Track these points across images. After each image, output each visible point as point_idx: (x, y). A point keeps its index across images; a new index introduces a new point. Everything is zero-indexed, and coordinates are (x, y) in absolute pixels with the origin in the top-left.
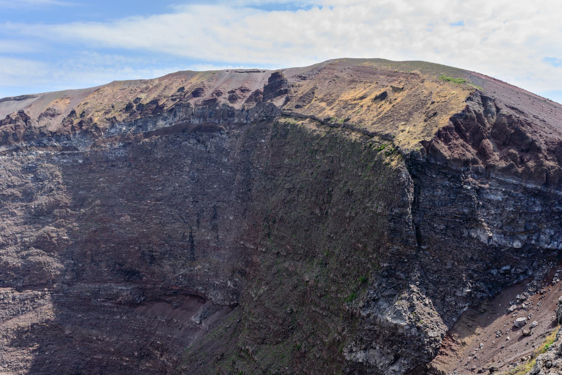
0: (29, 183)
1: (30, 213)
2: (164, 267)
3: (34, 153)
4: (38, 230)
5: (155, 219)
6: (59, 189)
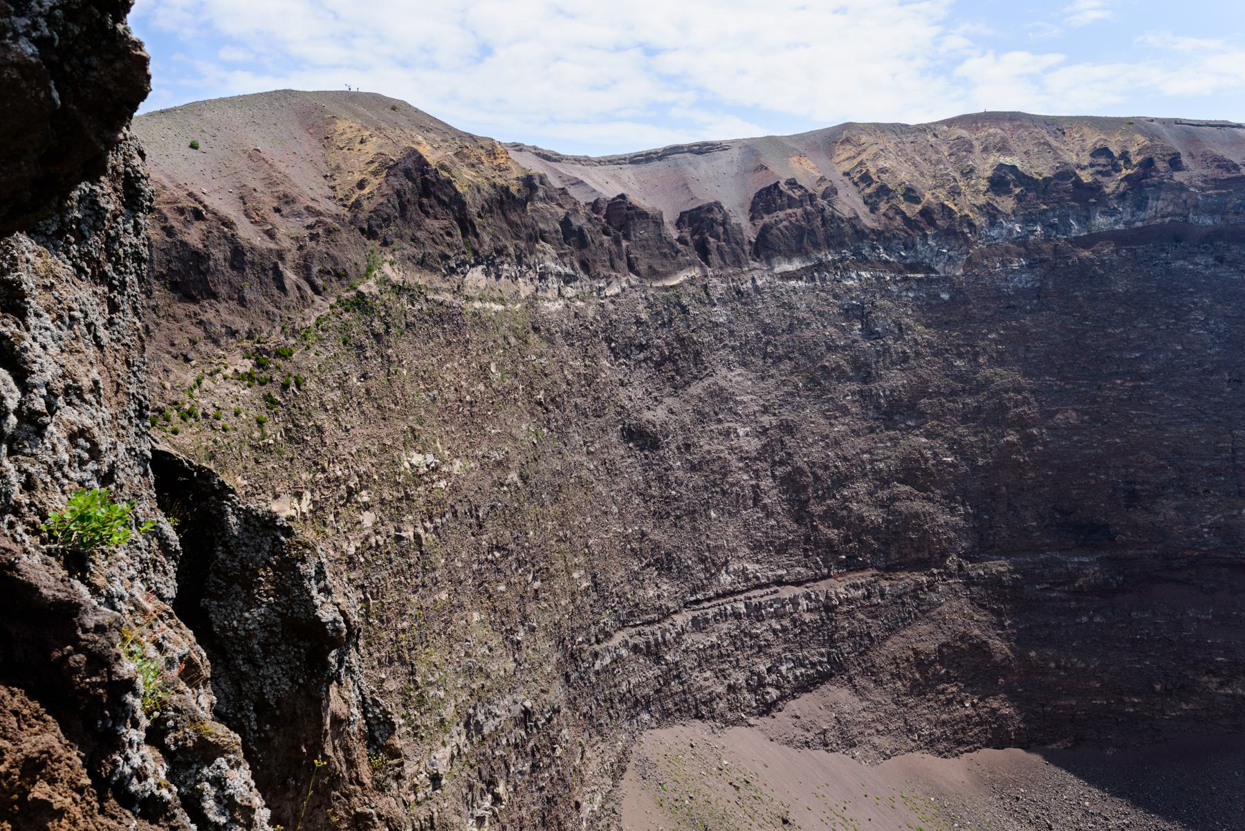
0: (856, 341)
1: (878, 407)
2: (1157, 514)
3: (854, 275)
5: (1139, 416)
6: (918, 354)
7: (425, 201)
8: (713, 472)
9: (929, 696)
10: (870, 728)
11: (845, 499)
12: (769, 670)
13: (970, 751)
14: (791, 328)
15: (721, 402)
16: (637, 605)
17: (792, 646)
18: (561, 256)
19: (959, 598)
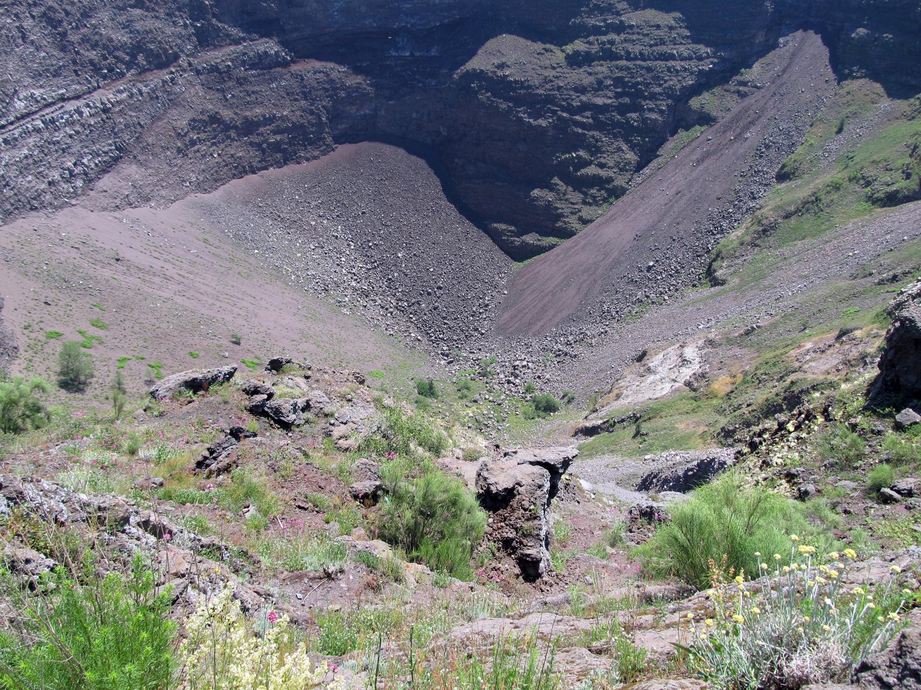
10: (157, 186)
12: (75, 164)
19: (194, 85)
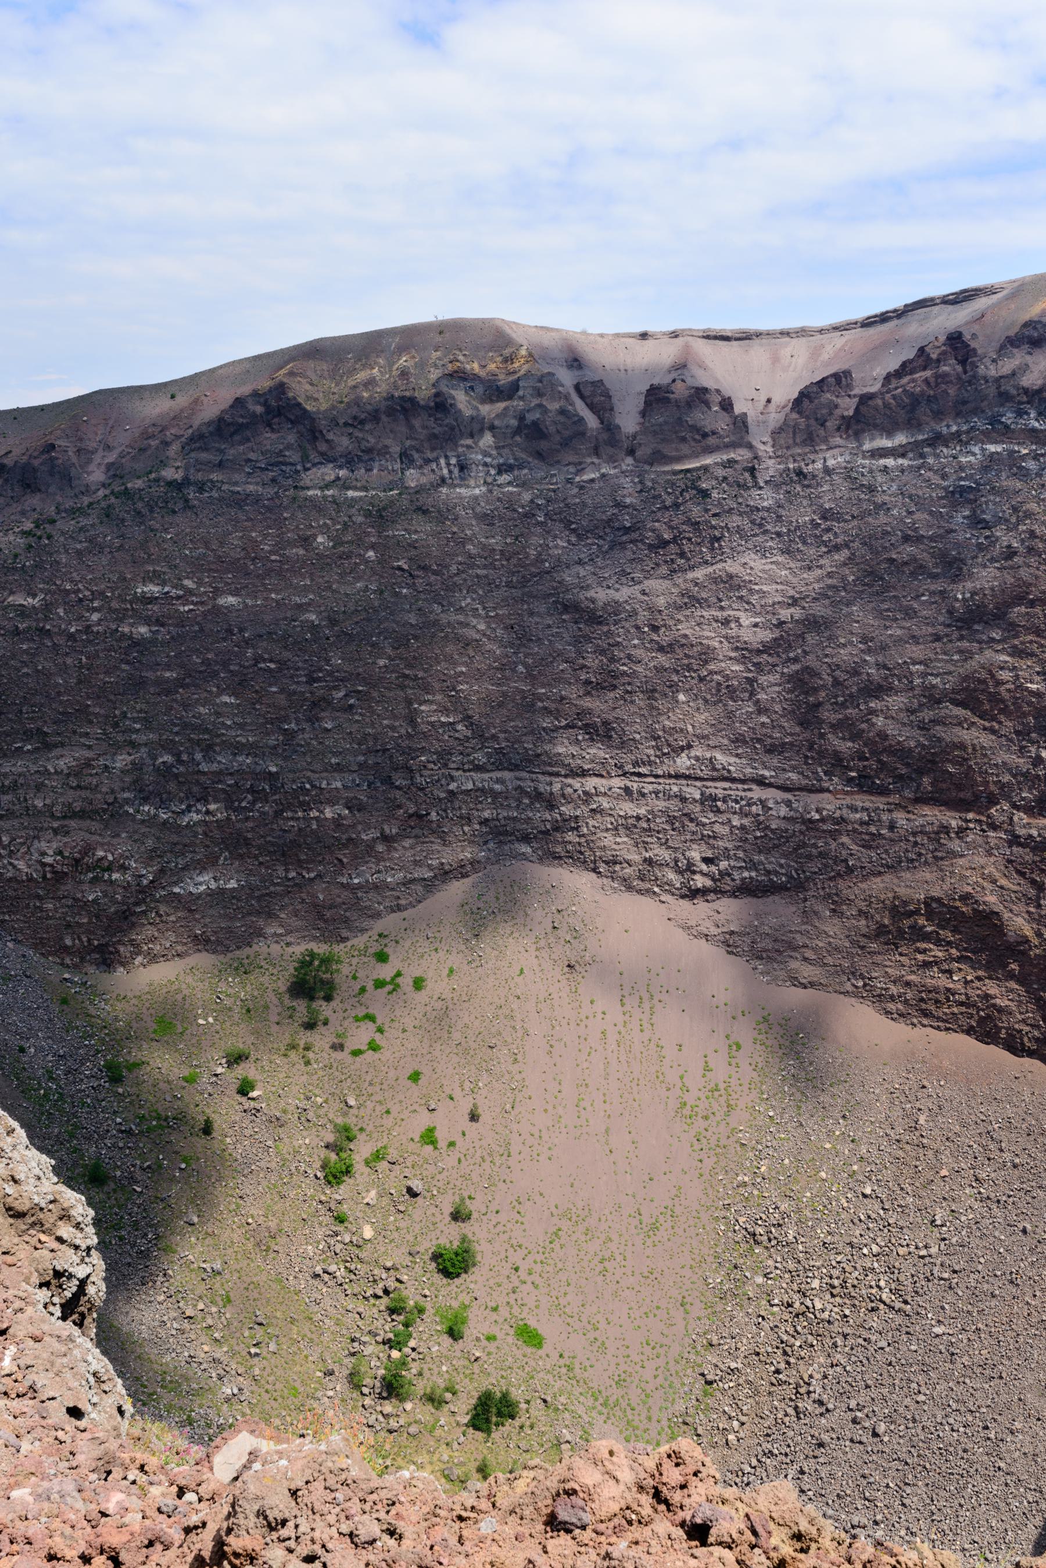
0: (955, 531)
1: (950, 612)
3: (976, 450)
4: (965, 660)
7: (276, 420)
8: (687, 656)
9: (903, 949)
10: (795, 949)
11: (872, 712)
12: (707, 861)
13: (938, 1028)
14: (861, 516)
15: (732, 588)
16: (538, 755)
17: (748, 846)
18: (497, 448)
19: (991, 855)
